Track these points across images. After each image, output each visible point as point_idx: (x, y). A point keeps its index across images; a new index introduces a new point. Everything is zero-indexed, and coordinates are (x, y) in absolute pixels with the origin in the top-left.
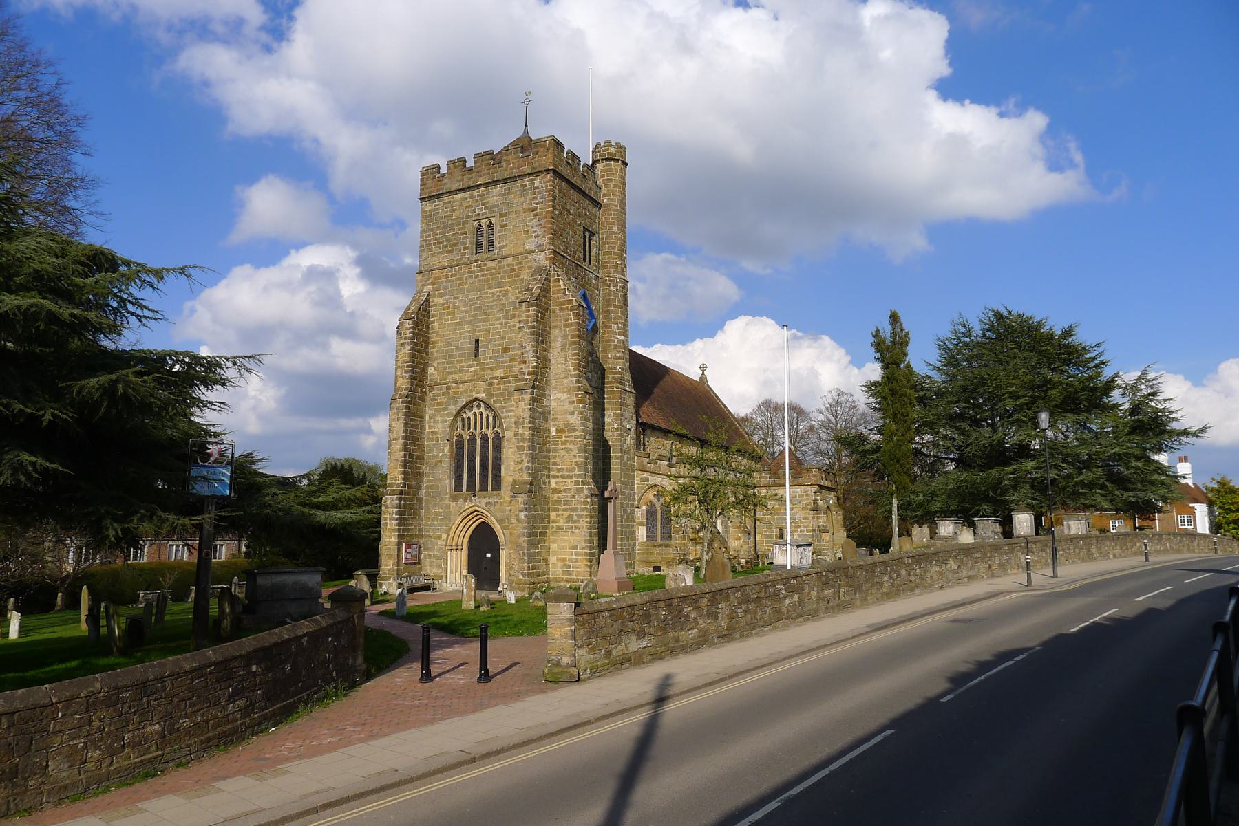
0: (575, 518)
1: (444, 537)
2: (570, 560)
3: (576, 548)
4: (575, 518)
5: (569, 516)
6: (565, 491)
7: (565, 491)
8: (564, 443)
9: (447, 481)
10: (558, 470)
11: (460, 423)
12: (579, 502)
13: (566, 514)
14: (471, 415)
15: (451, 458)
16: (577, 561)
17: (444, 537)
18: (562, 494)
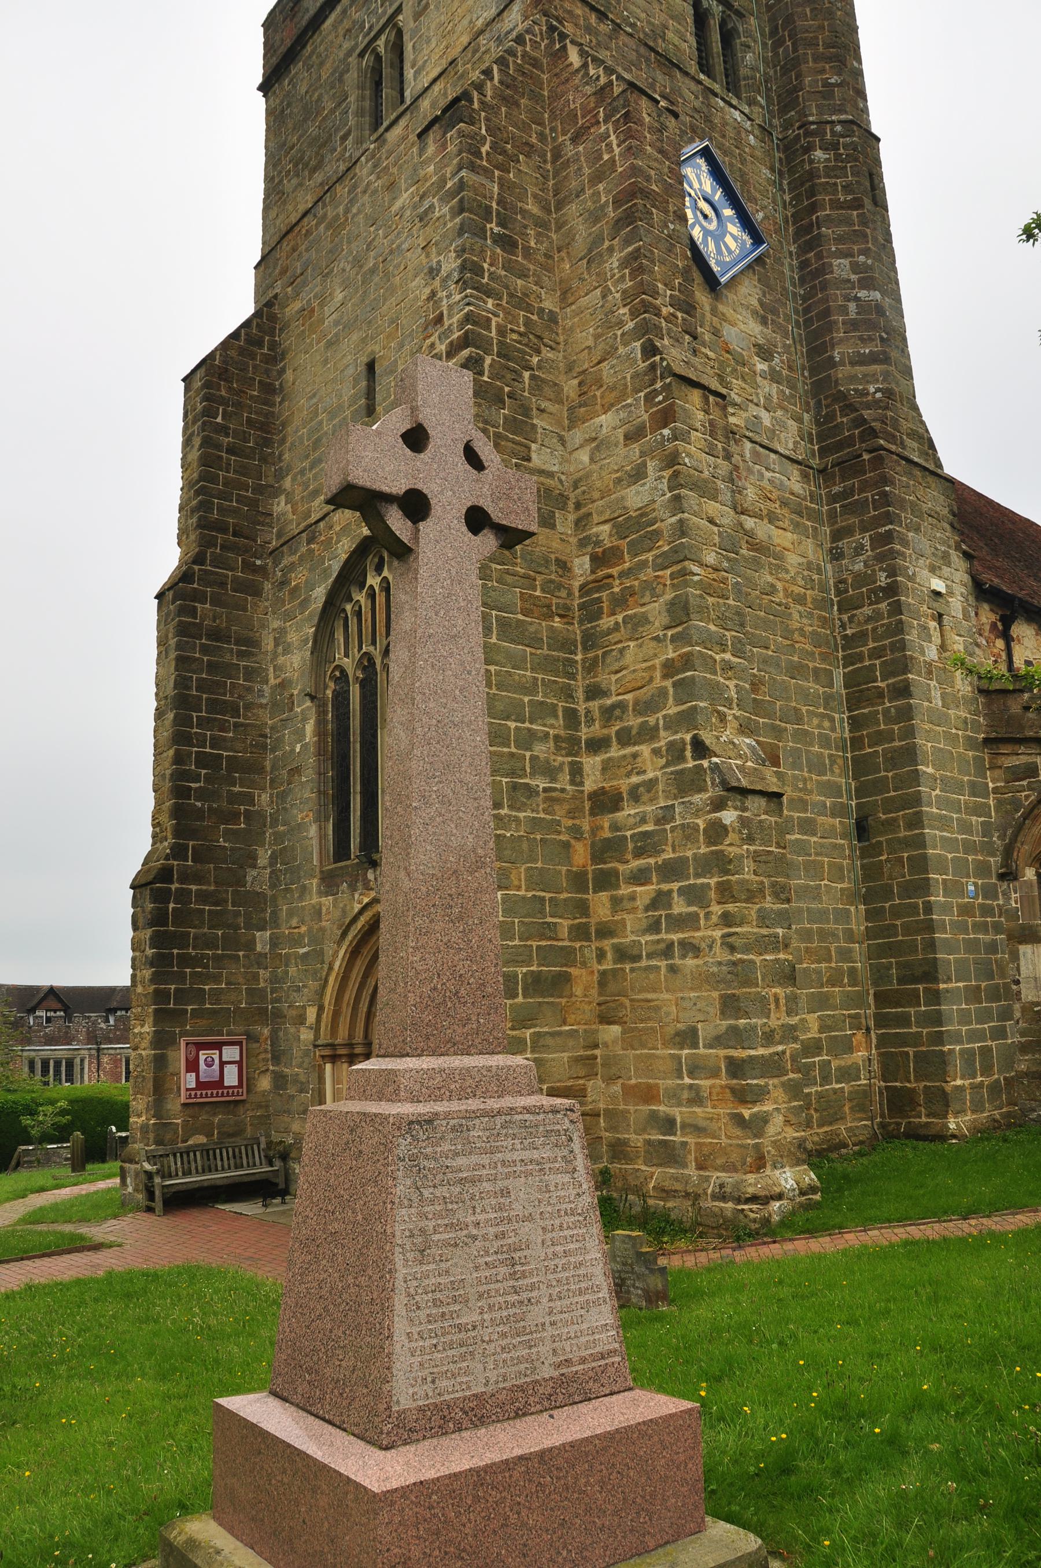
0: (679, 907)
1: (311, 1014)
4: (679, 907)
5: (660, 900)
6: (635, 795)
7: (635, 795)
8: (620, 602)
9: (313, 831)
10: (609, 714)
11: (340, 636)
12: (689, 833)
13: (644, 892)
14: (361, 597)
15: (320, 752)
16: (697, 1099)
17: (311, 1014)
18: (628, 811)
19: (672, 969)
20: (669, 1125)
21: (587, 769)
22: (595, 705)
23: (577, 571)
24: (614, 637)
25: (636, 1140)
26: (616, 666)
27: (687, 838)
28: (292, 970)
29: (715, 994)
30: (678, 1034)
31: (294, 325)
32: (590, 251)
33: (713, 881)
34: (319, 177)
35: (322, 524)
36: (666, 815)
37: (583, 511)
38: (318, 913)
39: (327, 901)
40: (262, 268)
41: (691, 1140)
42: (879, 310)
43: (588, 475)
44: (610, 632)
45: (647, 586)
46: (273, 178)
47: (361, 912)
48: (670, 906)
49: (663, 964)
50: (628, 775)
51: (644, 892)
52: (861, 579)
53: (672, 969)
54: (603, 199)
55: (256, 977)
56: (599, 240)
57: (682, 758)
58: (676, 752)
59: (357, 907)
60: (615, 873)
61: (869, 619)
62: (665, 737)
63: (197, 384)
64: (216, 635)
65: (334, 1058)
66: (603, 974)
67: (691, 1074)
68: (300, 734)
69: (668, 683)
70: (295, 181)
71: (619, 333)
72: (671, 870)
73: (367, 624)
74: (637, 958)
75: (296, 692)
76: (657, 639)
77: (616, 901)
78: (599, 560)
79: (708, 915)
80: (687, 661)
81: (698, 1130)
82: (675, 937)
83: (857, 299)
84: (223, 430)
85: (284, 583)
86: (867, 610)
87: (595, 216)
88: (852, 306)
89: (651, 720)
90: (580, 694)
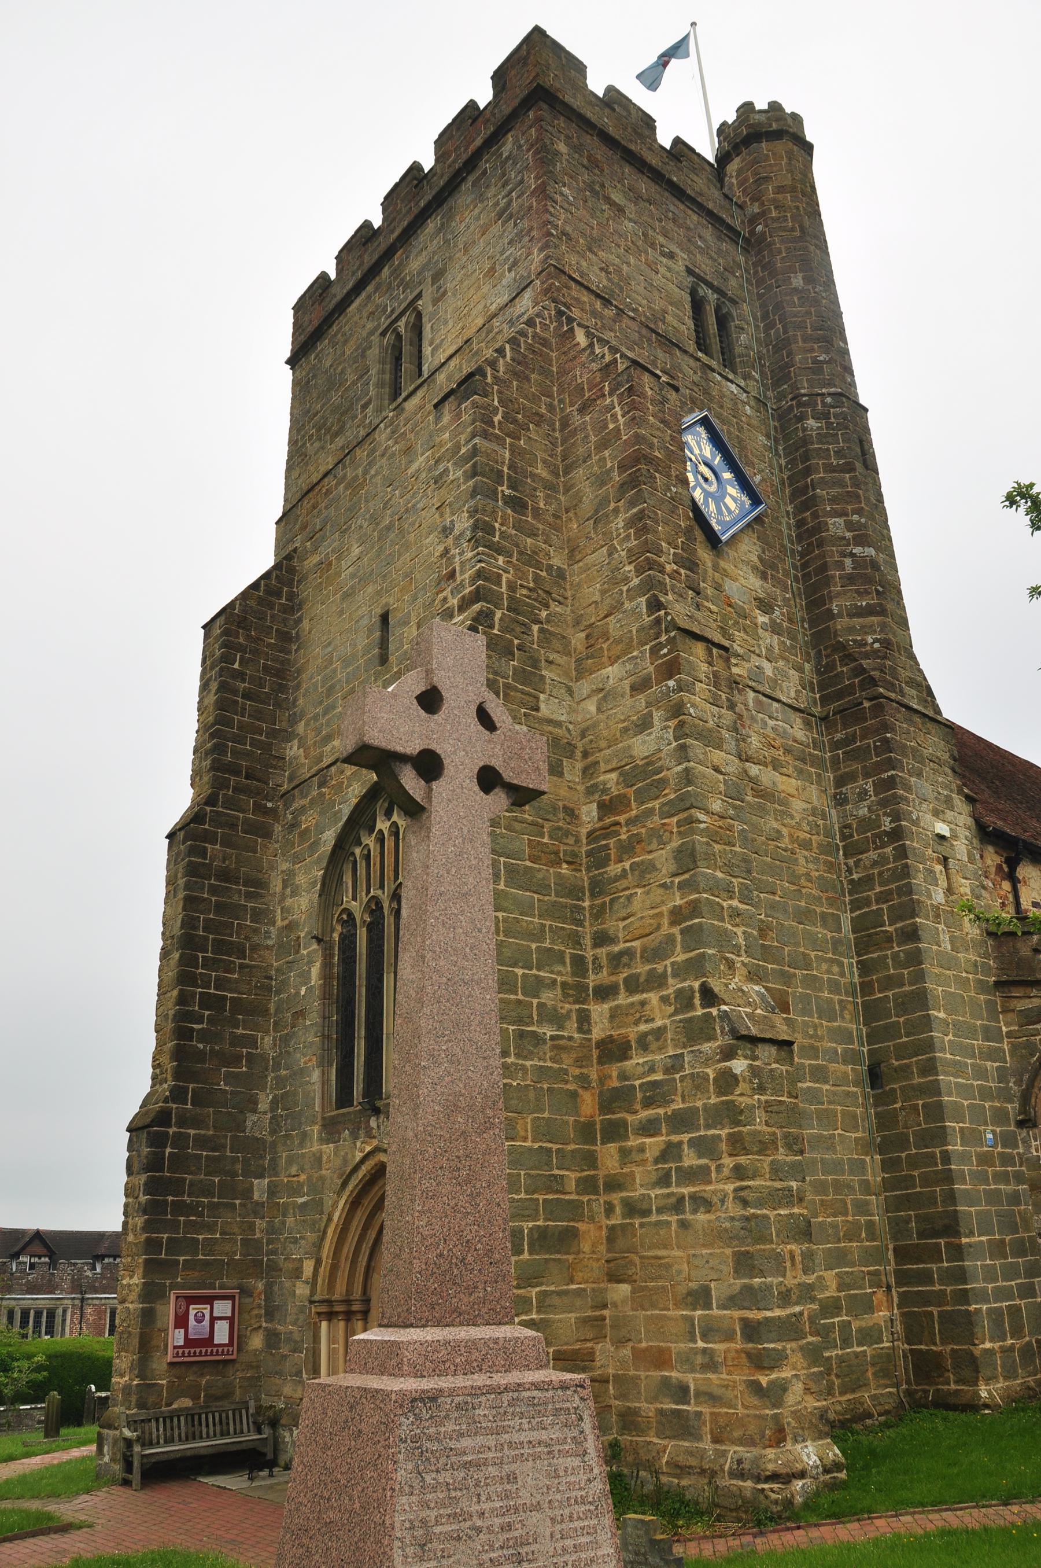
0: (690, 1159)
1: (308, 1267)
2: (687, 1361)
3: (701, 1297)
4: (690, 1159)
6: (643, 1043)
7: (643, 1043)
8: (627, 849)
9: (316, 1075)
10: (616, 961)
12: (699, 1082)
13: (654, 1144)
14: (370, 841)
15: (326, 995)
16: (711, 1365)
17: (308, 1267)
18: (637, 1060)
19: (684, 1225)
20: (682, 1392)
21: (594, 1016)
22: (602, 952)
23: (585, 818)
24: (623, 883)
25: (648, 1409)
26: (623, 913)
27: (697, 1088)
28: (290, 1221)
29: (728, 1251)
30: (690, 1293)
31: (311, 577)
32: (597, 512)
33: (724, 1133)
34: (340, 441)
35: (333, 769)
36: (675, 1064)
37: (591, 759)
38: (318, 1160)
39: (328, 1149)
40: (283, 524)
41: (705, 1410)
42: (874, 565)
43: (595, 725)
44: (617, 878)
45: (654, 833)
46: (297, 441)
47: (363, 1161)
48: (680, 1158)
49: (673, 1219)
50: (637, 1023)
51: (654, 1144)
52: (865, 824)
53: (684, 1225)
54: (609, 465)
55: (252, 1227)
56: (605, 501)
57: (690, 1006)
58: (684, 1000)
59: (359, 1156)
60: (625, 1123)
61: (875, 863)
62: (674, 985)
63: (217, 631)
64: (225, 875)
65: (330, 1316)
66: (612, 1229)
67: (705, 1337)
68: (305, 977)
69: (676, 930)
70: (317, 445)
71: (625, 588)
72: (681, 1121)
73: (376, 868)
74: (647, 1213)
75: (302, 935)
76: (664, 886)
77: (625, 1154)
78: (606, 808)
79: (719, 1168)
80: (695, 909)
81: (713, 1399)
82: (686, 1191)
83: (852, 555)
84: (240, 675)
85: (294, 825)
86: (873, 855)
87: (601, 480)
88: (848, 562)
89: (660, 968)
90: (588, 941)
